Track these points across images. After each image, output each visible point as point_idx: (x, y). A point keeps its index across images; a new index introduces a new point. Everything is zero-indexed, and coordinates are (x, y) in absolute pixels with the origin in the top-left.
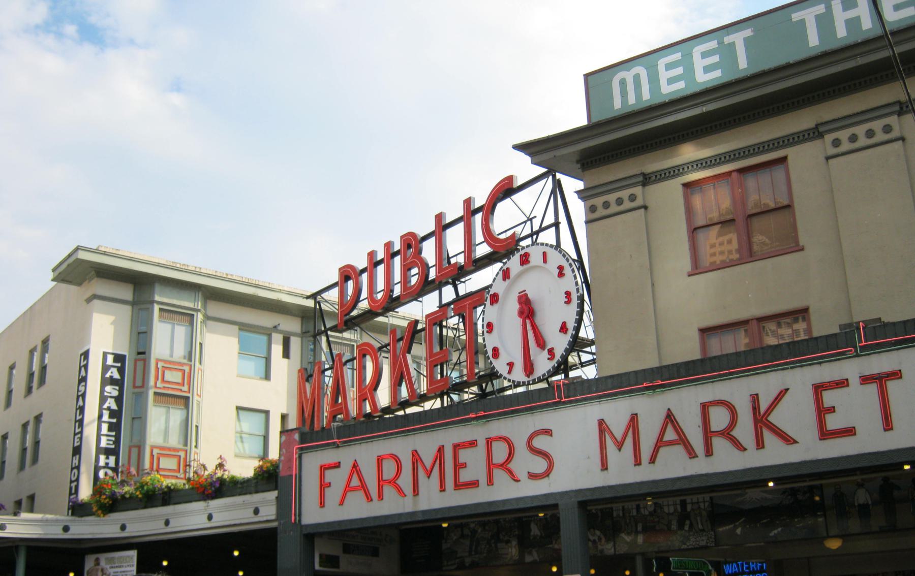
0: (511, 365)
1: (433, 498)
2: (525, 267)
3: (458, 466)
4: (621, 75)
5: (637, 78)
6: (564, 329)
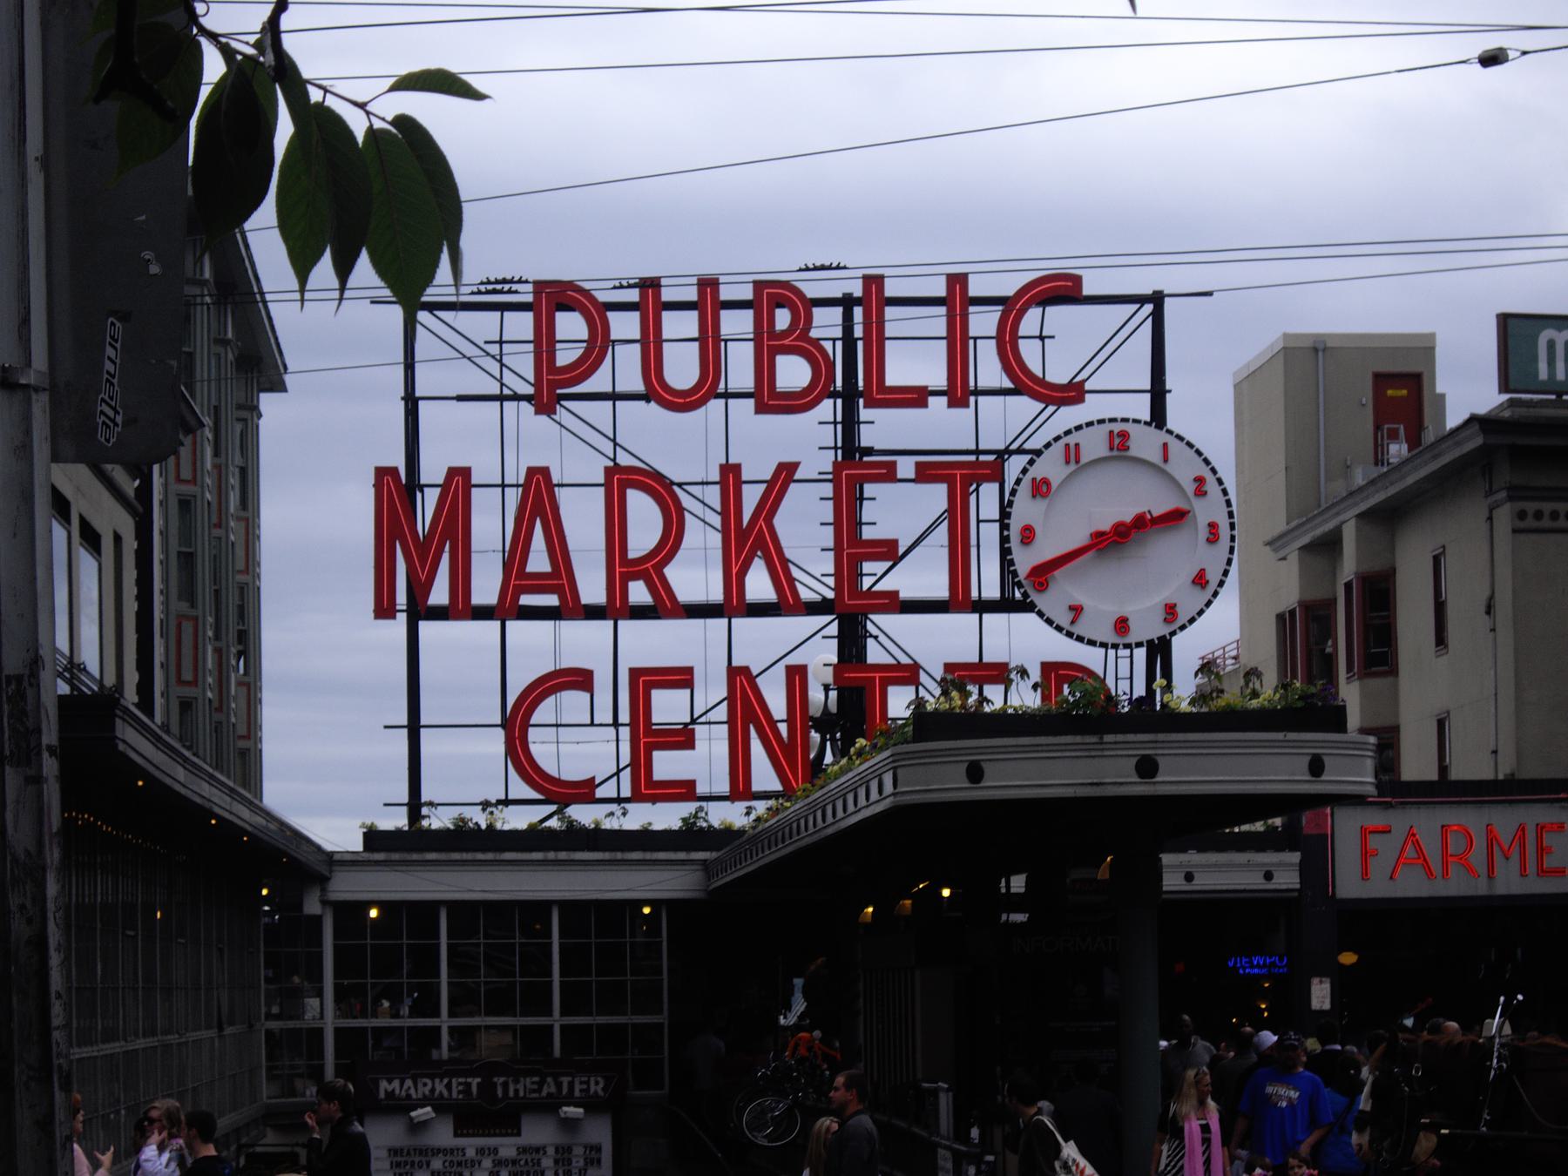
0: (1077, 610)
1: (1510, 881)
2: (1115, 453)
3: (1542, 851)
6: (1200, 580)
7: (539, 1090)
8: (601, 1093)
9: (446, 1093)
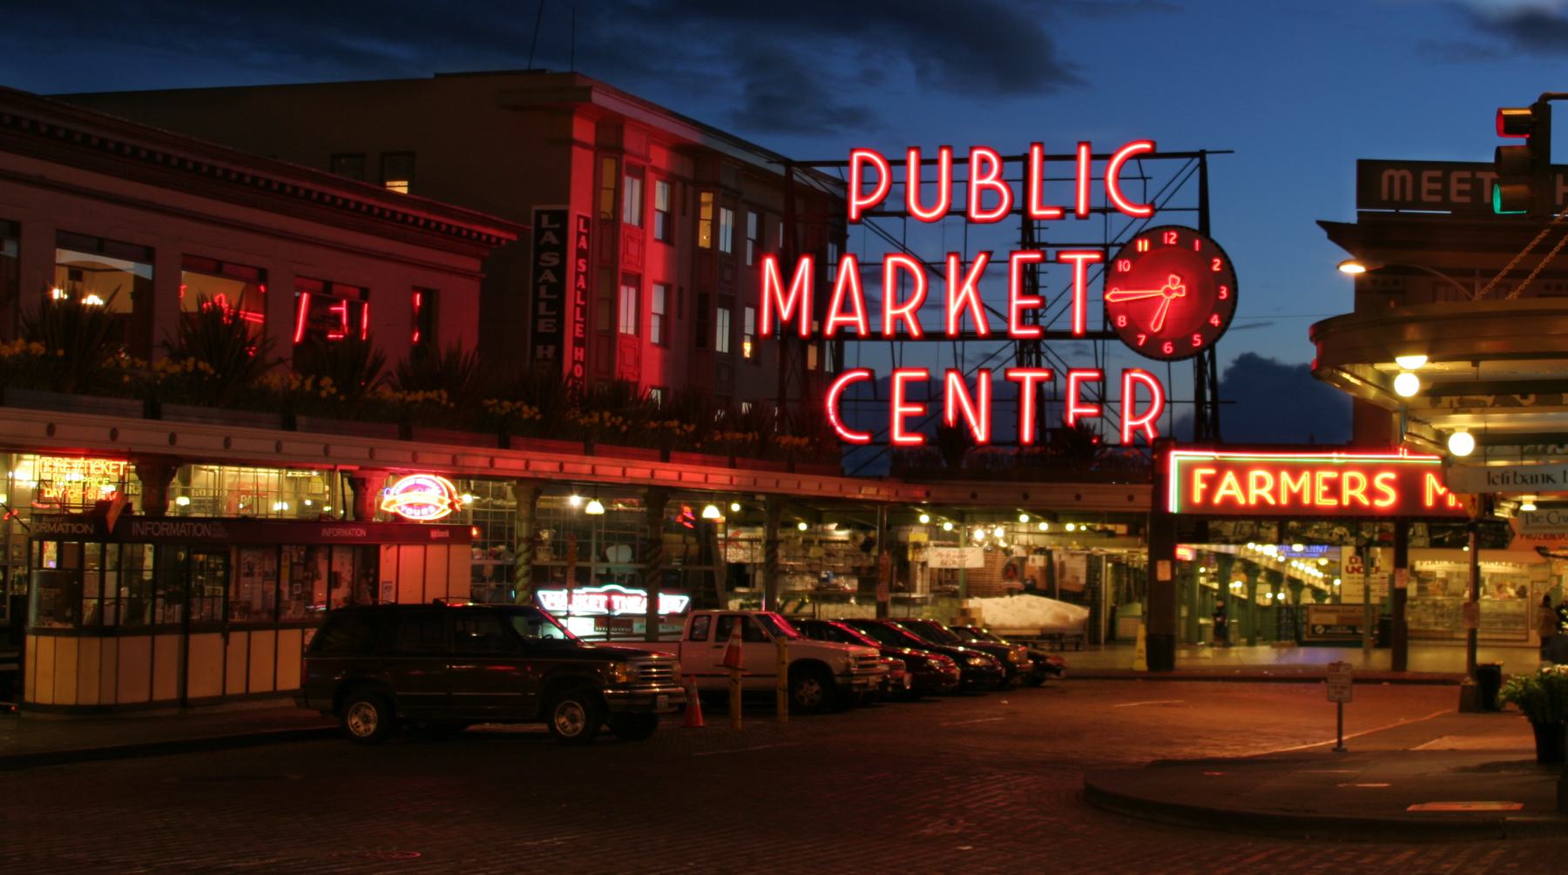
4: (1391, 172)
5: (1403, 179)
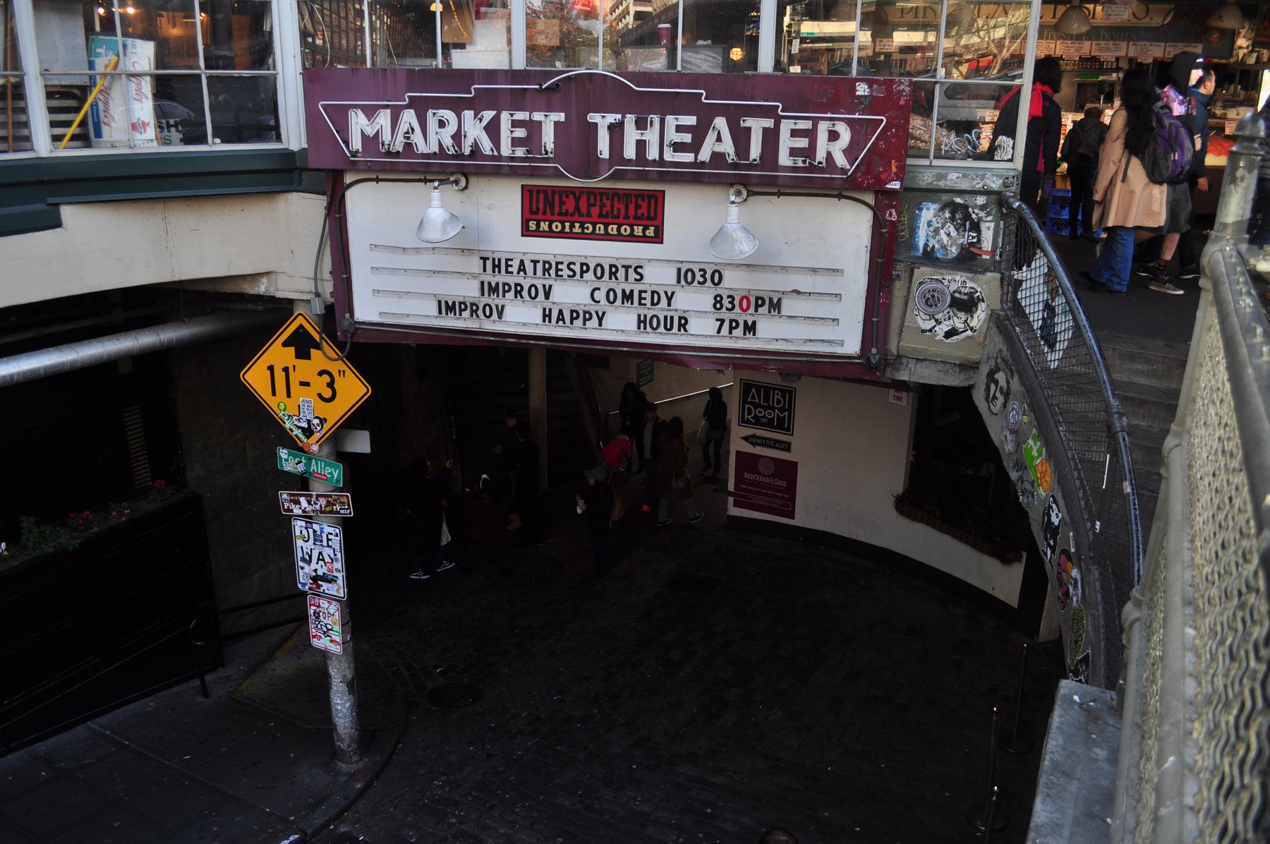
7: (695, 147)
8: (841, 161)
9: (487, 146)
